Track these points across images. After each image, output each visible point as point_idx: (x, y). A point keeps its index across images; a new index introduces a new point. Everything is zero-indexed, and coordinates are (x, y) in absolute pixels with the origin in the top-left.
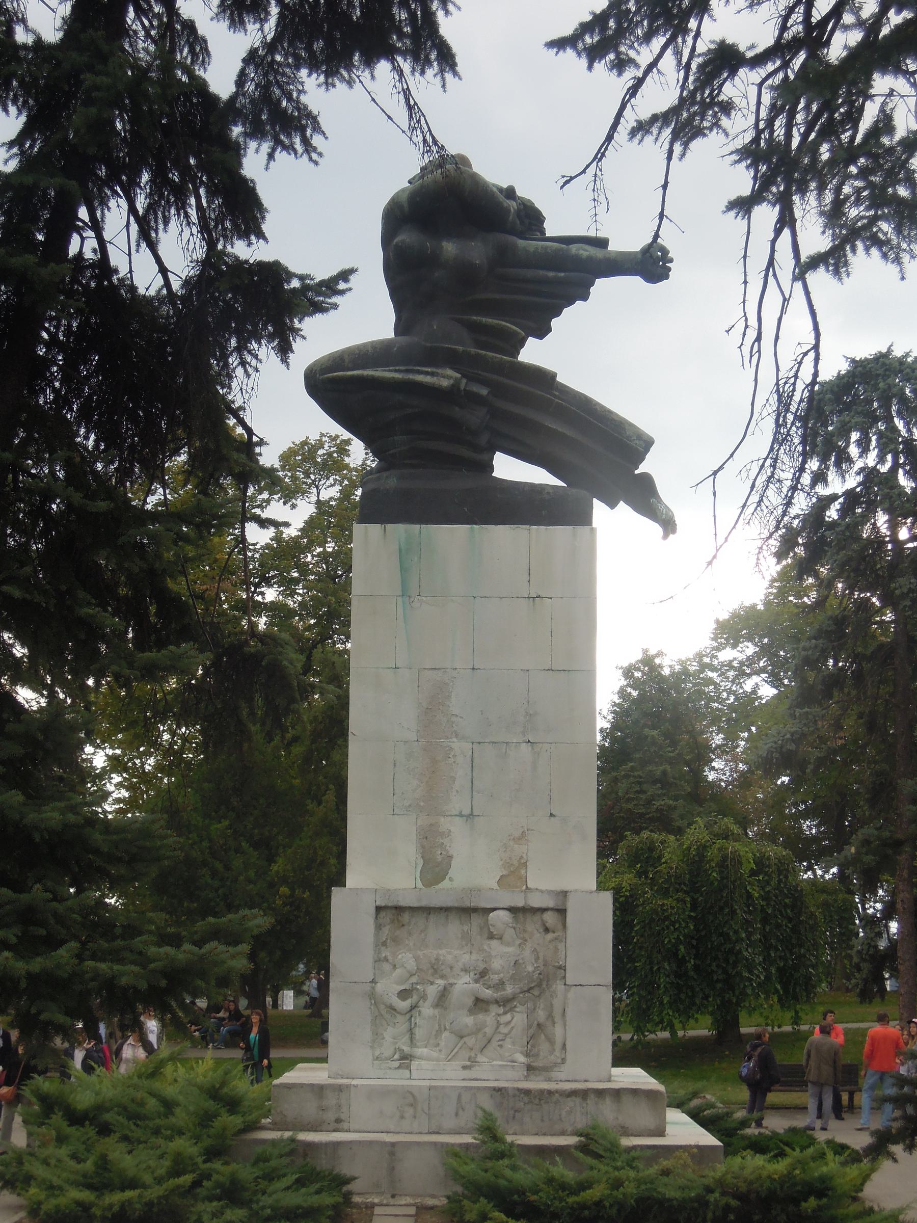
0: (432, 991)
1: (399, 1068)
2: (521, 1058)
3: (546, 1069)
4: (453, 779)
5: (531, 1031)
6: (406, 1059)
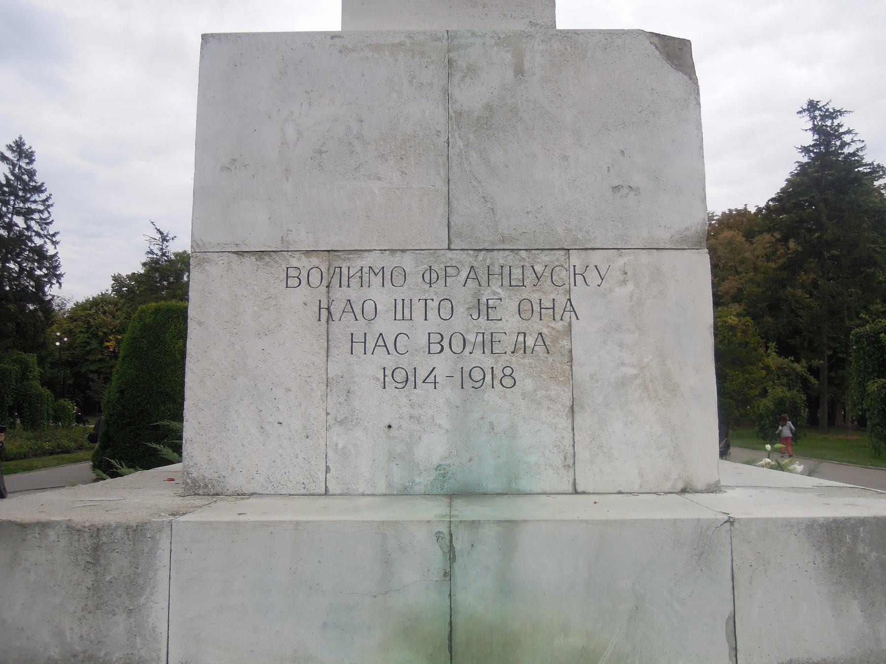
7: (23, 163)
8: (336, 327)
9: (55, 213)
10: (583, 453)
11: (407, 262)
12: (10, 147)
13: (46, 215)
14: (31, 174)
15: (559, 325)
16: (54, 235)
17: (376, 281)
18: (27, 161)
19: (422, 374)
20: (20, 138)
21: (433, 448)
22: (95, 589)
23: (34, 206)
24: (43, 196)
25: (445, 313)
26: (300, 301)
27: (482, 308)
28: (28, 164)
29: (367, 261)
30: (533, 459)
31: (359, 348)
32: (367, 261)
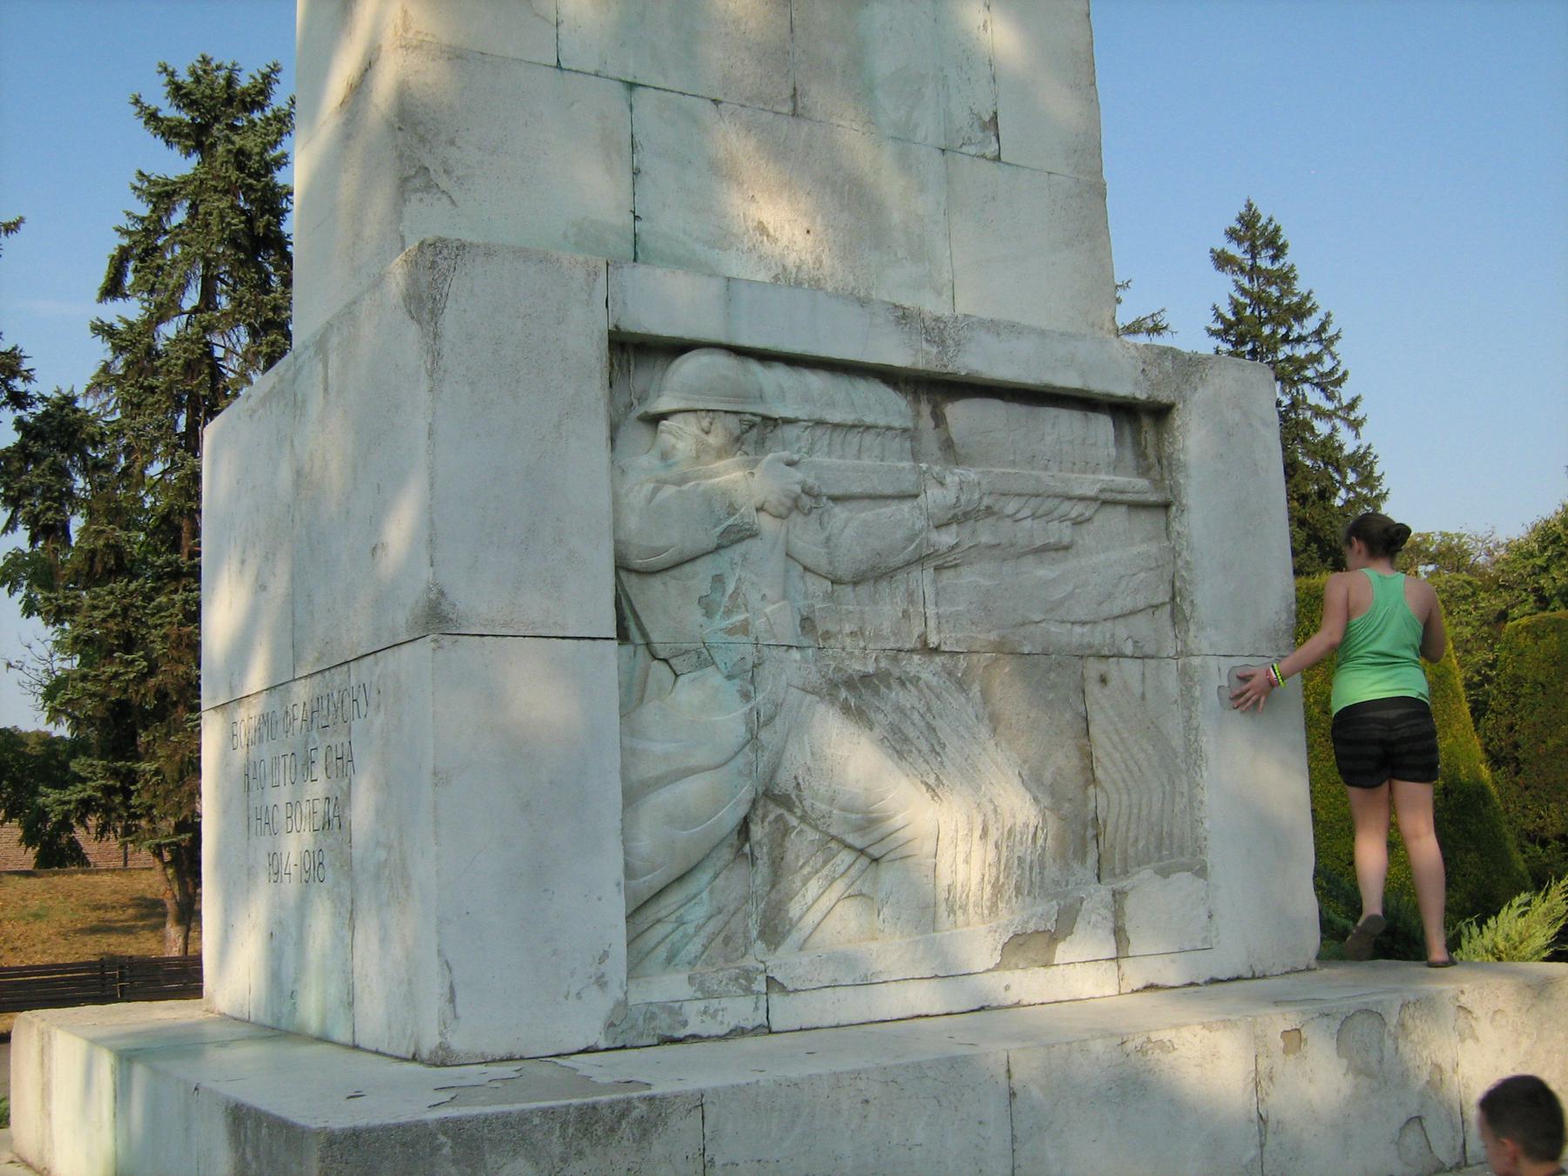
7: (1264, 263)
9: (1346, 353)
12: (1232, 234)
13: (1328, 364)
14: (1285, 278)
16: (1352, 406)
18: (1271, 253)
20: (1249, 206)
23: (1301, 351)
24: (1311, 324)
28: (1274, 258)
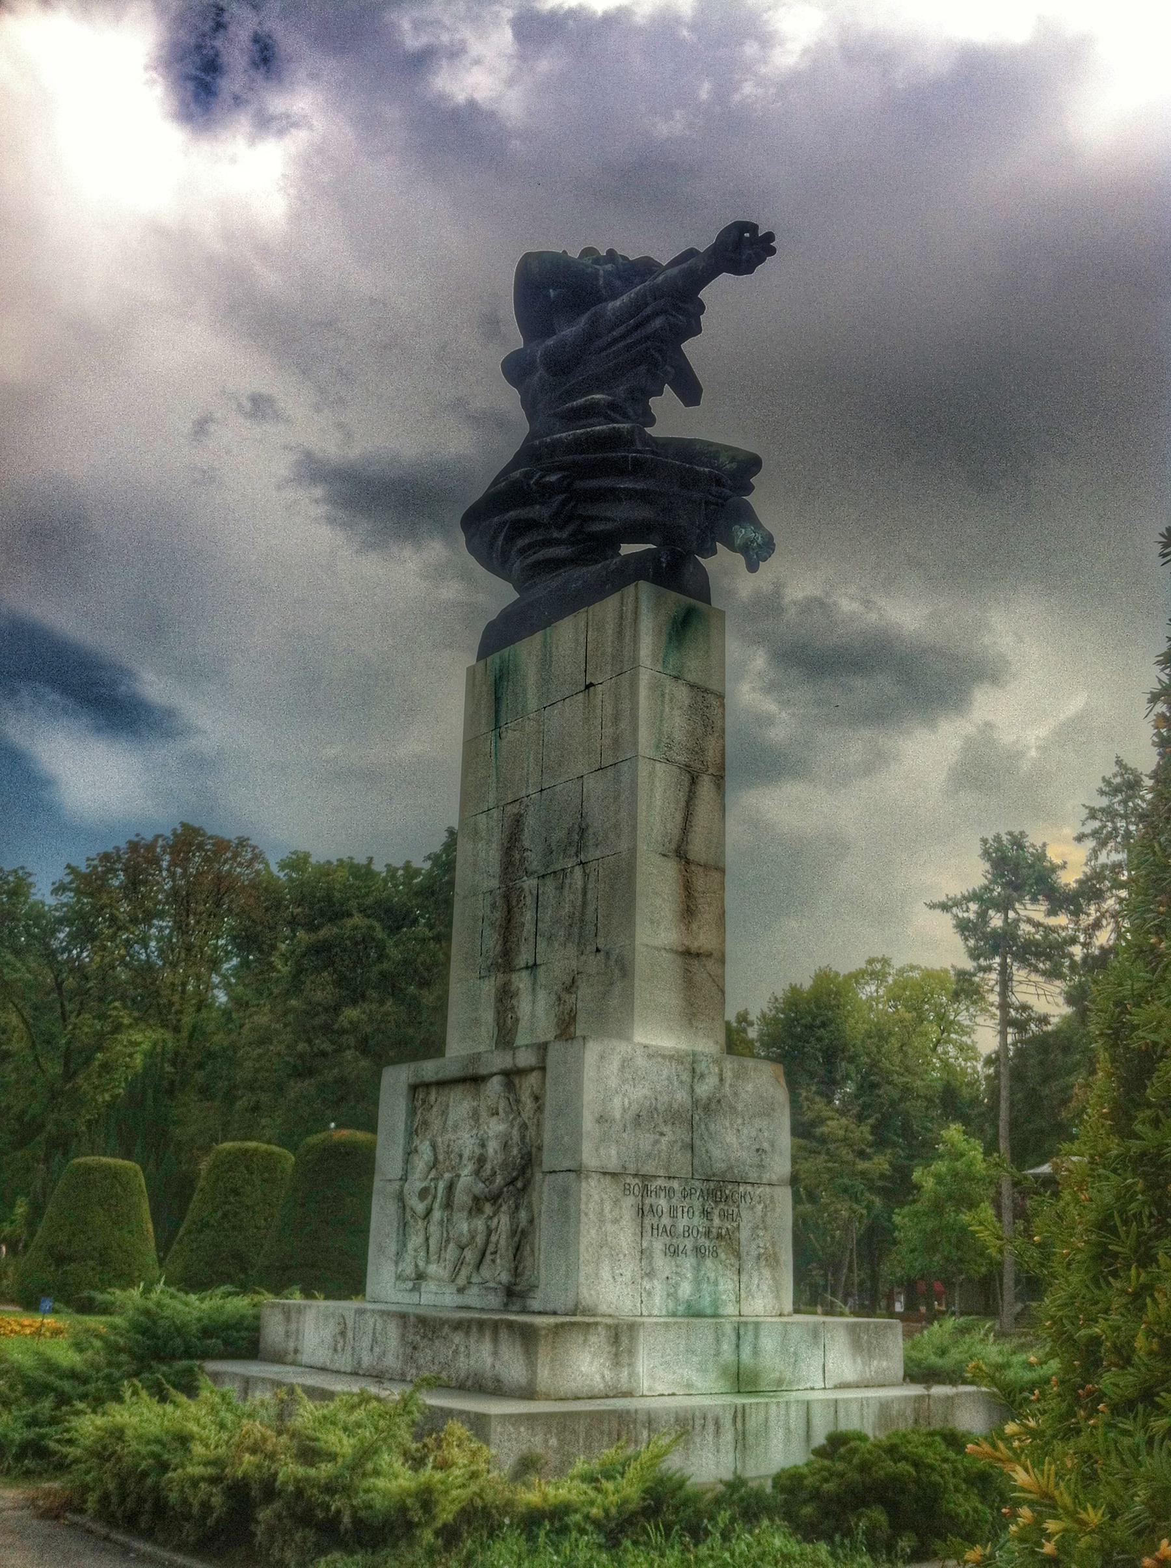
0: (441, 1185)
1: (411, 1290)
2: (505, 1277)
3: (523, 1296)
4: (523, 924)
5: (516, 1239)
6: (420, 1276)
8: (647, 1221)
10: (743, 1295)
11: (675, 1184)
15: (735, 1224)
17: (663, 1194)
19: (681, 1248)
21: (686, 1289)
22: (616, 1355)
25: (691, 1214)
26: (629, 1202)
27: (706, 1214)
29: (660, 1182)
30: (724, 1297)
31: (655, 1232)
32: (660, 1182)
